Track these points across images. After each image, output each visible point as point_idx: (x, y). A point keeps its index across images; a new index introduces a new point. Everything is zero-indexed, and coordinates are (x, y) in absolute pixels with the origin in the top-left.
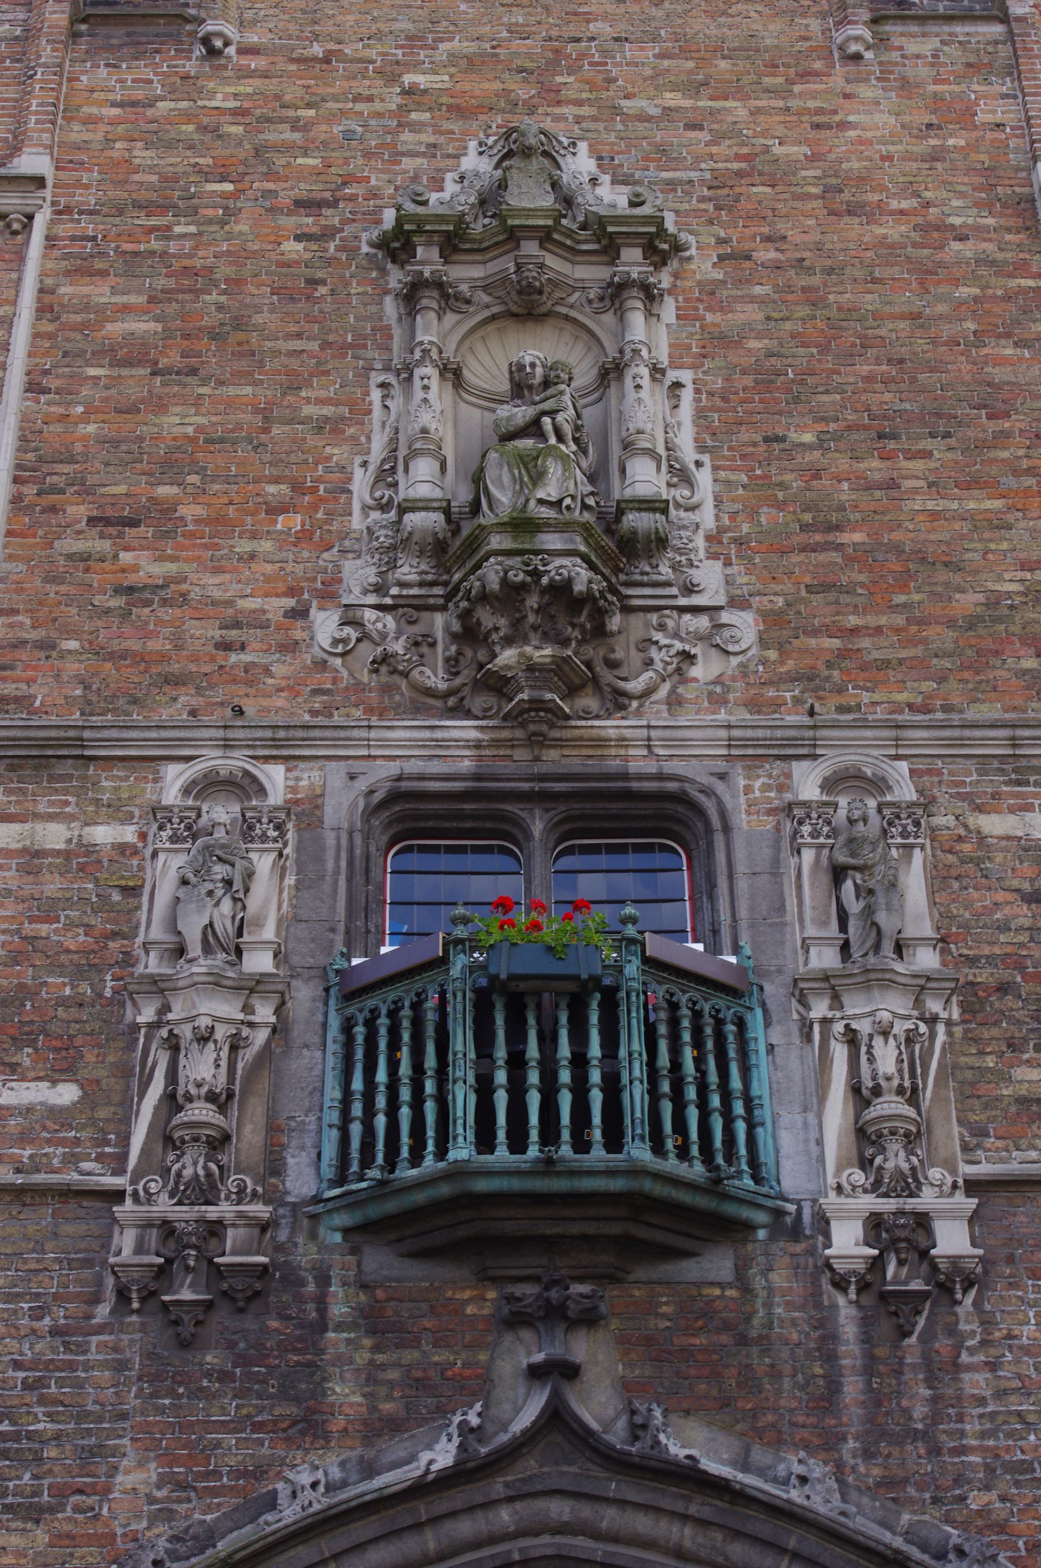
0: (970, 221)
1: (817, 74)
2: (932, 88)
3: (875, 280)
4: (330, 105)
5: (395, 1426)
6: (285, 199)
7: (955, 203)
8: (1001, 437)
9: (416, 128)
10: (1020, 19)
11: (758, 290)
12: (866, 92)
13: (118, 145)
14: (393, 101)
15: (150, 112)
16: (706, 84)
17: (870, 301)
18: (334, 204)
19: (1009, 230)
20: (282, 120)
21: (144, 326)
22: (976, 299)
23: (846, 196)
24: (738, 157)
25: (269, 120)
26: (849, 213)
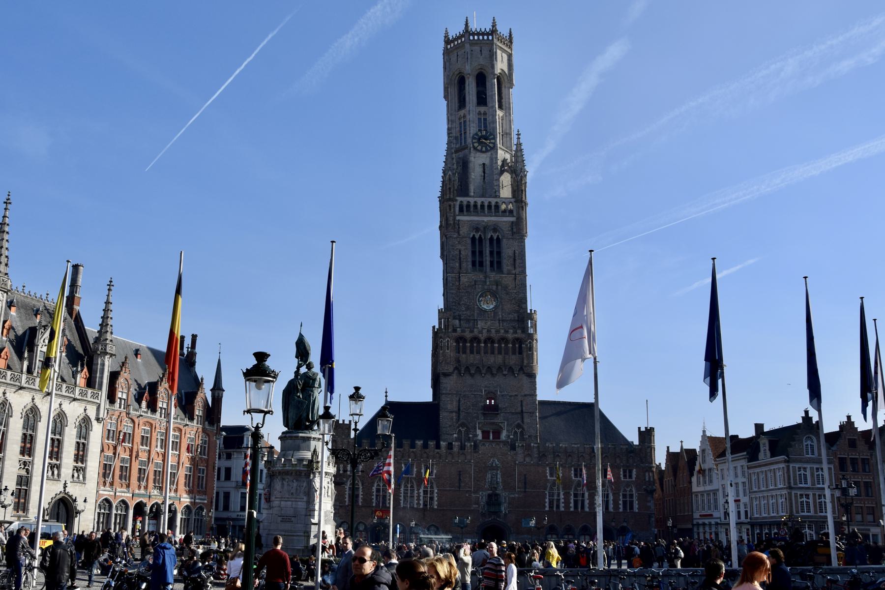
21: (477, 470)
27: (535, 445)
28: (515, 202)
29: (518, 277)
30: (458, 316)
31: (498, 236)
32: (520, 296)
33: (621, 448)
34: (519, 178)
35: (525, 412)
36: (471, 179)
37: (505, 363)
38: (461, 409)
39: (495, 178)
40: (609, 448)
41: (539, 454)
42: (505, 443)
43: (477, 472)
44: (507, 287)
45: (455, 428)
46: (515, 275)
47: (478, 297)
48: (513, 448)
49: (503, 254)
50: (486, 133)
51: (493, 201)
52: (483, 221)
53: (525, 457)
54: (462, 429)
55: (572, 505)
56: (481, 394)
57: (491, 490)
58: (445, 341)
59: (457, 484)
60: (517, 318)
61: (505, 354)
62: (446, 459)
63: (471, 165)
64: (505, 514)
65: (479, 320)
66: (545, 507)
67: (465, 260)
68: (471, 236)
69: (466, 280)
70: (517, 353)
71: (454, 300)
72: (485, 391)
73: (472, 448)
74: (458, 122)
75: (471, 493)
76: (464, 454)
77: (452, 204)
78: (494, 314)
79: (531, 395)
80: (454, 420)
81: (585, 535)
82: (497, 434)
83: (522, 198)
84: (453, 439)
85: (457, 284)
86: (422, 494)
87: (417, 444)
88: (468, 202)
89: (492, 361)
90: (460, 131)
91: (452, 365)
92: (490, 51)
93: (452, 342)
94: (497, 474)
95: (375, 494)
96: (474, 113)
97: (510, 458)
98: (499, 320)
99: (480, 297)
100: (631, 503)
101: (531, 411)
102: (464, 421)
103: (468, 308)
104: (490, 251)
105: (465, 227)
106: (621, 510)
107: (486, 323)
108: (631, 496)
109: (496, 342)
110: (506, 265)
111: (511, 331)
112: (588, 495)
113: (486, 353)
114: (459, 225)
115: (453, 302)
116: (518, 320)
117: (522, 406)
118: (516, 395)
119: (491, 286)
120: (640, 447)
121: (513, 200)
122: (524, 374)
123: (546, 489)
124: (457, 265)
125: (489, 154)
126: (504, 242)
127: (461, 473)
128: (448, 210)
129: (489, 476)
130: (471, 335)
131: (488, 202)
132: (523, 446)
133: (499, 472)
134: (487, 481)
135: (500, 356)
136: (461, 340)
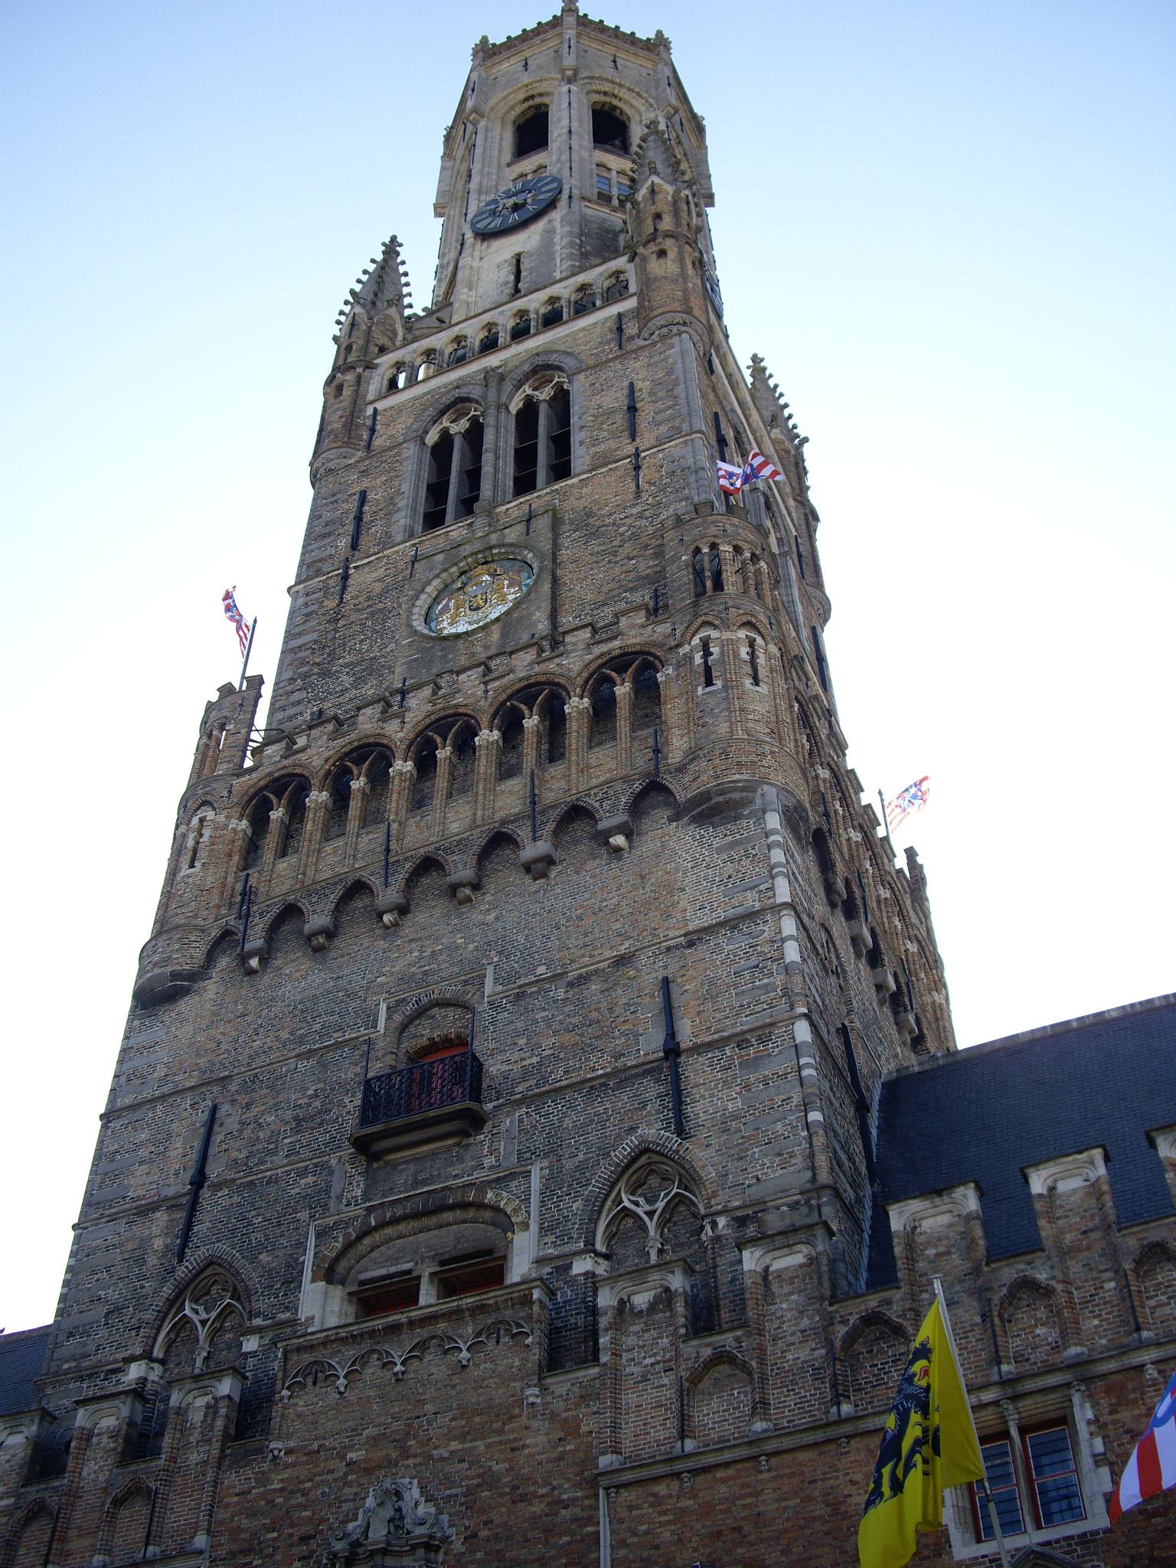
0: (571, 1495)
1: (515, 1417)
2: (565, 1415)
3: (527, 1541)
4: (318, 1478)
6: (296, 1538)
7: (566, 1486)
9: (349, 1484)
10: (605, 1364)
11: (479, 1555)
12: (535, 1424)
13: (236, 1518)
15: (249, 1497)
16: (468, 1433)
18: (313, 1537)
19: (587, 1497)
20: (298, 1491)
22: (569, 1543)
23: (520, 1491)
24: (479, 1476)
25: (293, 1492)
26: (521, 1501)
28: (631, 260)
35: (698, 1049)
37: (534, 795)
38: (215, 1170)
41: (824, 1332)
44: (590, 514)
45: (149, 1315)
46: (637, 455)
53: (688, 1390)
67: (381, 514)
68: (432, 438)
73: (220, 1423)
78: (504, 627)
79: (731, 924)
80: (152, 1261)
85: (331, 604)
93: (221, 818)
99: (436, 600)
101: (746, 1022)
102: (223, 1248)
109: (484, 720)
111: (586, 634)
114: (374, 424)
115: (293, 680)
117: (668, 1011)
118: (622, 961)
121: (620, 262)
122: (675, 818)
124: (343, 543)
125: (540, 225)
128: (331, 400)
132: (667, 1297)
135: (515, 784)
136: (279, 796)
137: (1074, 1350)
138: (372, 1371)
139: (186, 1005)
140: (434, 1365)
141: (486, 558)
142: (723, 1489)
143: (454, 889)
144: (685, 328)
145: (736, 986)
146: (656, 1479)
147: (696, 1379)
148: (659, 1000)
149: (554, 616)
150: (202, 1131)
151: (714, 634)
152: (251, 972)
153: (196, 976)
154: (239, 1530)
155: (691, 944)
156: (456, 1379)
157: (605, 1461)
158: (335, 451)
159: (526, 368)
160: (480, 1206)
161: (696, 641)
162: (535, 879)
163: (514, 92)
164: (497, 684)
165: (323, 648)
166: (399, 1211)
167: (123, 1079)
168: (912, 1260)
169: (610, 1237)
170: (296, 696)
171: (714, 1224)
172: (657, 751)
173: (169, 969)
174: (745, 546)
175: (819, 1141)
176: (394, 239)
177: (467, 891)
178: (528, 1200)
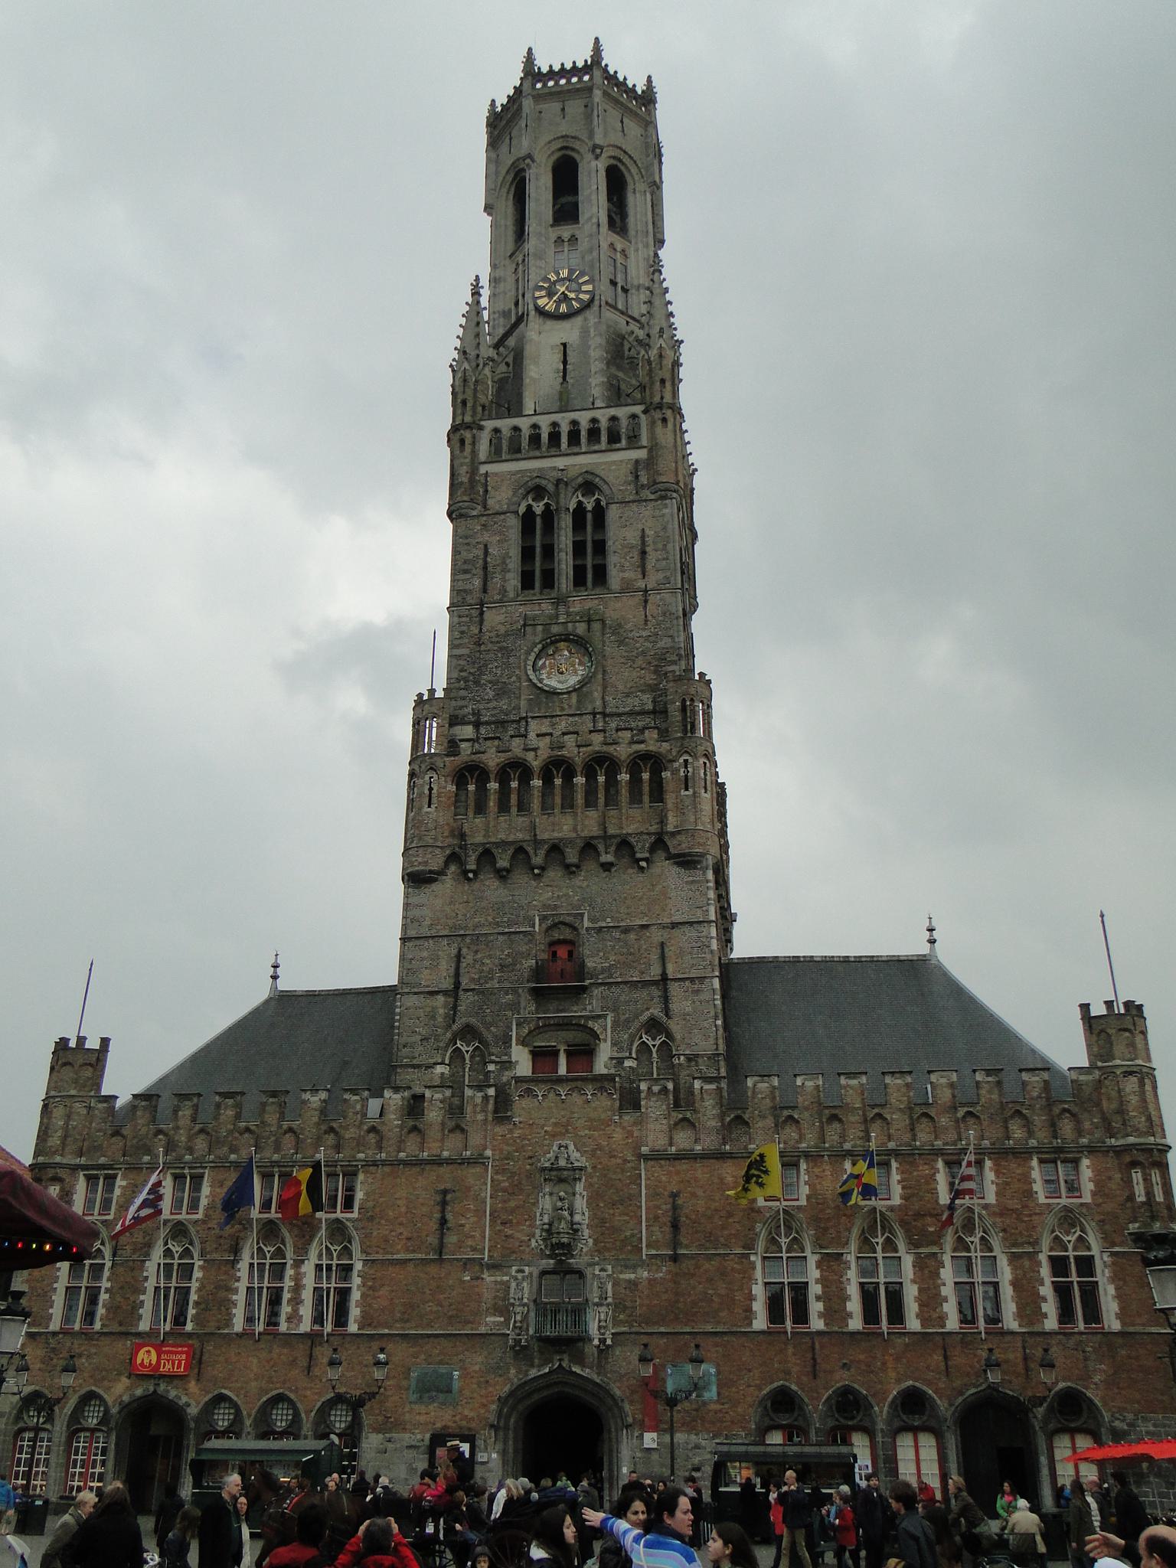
5: (542, 1365)
8: (631, 1205)
9: (546, 1139)
12: (617, 1130)
14: (543, 1133)
17: (614, 1177)
27: (707, 1087)
28: (645, 412)
29: (653, 598)
30: (474, 714)
31: (598, 501)
32: (661, 644)
33: (1024, 1084)
34: (653, 353)
36: (527, 381)
37: (606, 828)
38: (465, 982)
39: (593, 371)
40: (978, 1083)
41: (722, 1117)
42: (603, 1082)
43: (504, 1190)
44: (620, 625)
46: (646, 591)
47: (532, 657)
48: (631, 1101)
49: (610, 543)
50: (571, 272)
51: (584, 418)
52: (554, 468)
54: (464, 1049)
55: (854, 1305)
56: (528, 929)
57: (550, 1257)
58: (420, 781)
59: (433, 1240)
60: (650, 707)
61: (606, 805)
62: (399, 1152)
63: (529, 351)
64: (604, 1350)
65: (533, 718)
66: (749, 1314)
67: (499, 569)
68: (522, 509)
69: (501, 618)
70: (646, 798)
71: (464, 674)
72: (543, 919)
73: (491, 1107)
74: (511, 279)
75: (483, 1273)
76: (463, 1130)
77: (468, 435)
78: (578, 696)
79: (691, 923)
81: (915, 1430)
82: (583, 1053)
83: (662, 398)
84: (431, 1079)
86: (309, 1281)
87: (304, 1102)
88: (516, 429)
89: (565, 827)
90: (517, 296)
91: (441, 848)
92: (586, 106)
94: (574, 1194)
95: (150, 1285)
96: (544, 239)
97: (618, 1135)
98: (594, 714)
99: (538, 657)
100: (1090, 1294)
102: (473, 1021)
103: (502, 691)
104: (574, 542)
105: (504, 488)
106: (1051, 1323)
107: (553, 725)
108: (1086, 1265)
109: (579, 769)
110: (619, 568)
111: (628, 734)
112: (913, 1262)
113: (547, 808)
114: (486, 486)
115: (458, 680)
116: (654, 712)
119: (570, 624)
120: (1097, 1074)
121: (638, 409)
123: (750, 1246)
124: (477, 582)
125: (578, 321)
126: (613, 514)
127: (449, 1197)
128: (458, 452)
129: (546, 1203)
130: (502, 758)
131: (567, 421)
132: (665, 1090)
133: (579, 1187)
134: (538, 1223)
135: (593, 814)
137: (804, 1145)
138: (552, 1095)
139: (434, 886)
140: (576, 1098)
141: (566, 638)
142: (685, 1167)
143: (567, 867)
144: (675, 495)
145: (690, 953)
146: (661, 1159)
147: (676, 1124)
148: (659, 951)
149: (603, 698)
150: (455, 959)
151: (690, 760)
152: (469, 879)
153: (442, 873)
154: (501, 1150)
155: (673, 928)
156: (586, 1106)
157: (644, 1150)
158: (466, 504)
159: (580, 480)
160: (585, 1027)
161: (681, 760)
162: (605, 871)
163: (555, 139)
164: (585, 749)
165: (474, 663)
166: (552, 1022)
167: (409, 920)
168: (753, 1098)
169: (637, 1051)
170: (463, 693)
171: (679, 1059)
172: (662, 822)
173: (428, 868)
174: (705, 701)
175: (721, 1031)
176: (477, 278)
177: (574, 869)
178: (606, 1030)
